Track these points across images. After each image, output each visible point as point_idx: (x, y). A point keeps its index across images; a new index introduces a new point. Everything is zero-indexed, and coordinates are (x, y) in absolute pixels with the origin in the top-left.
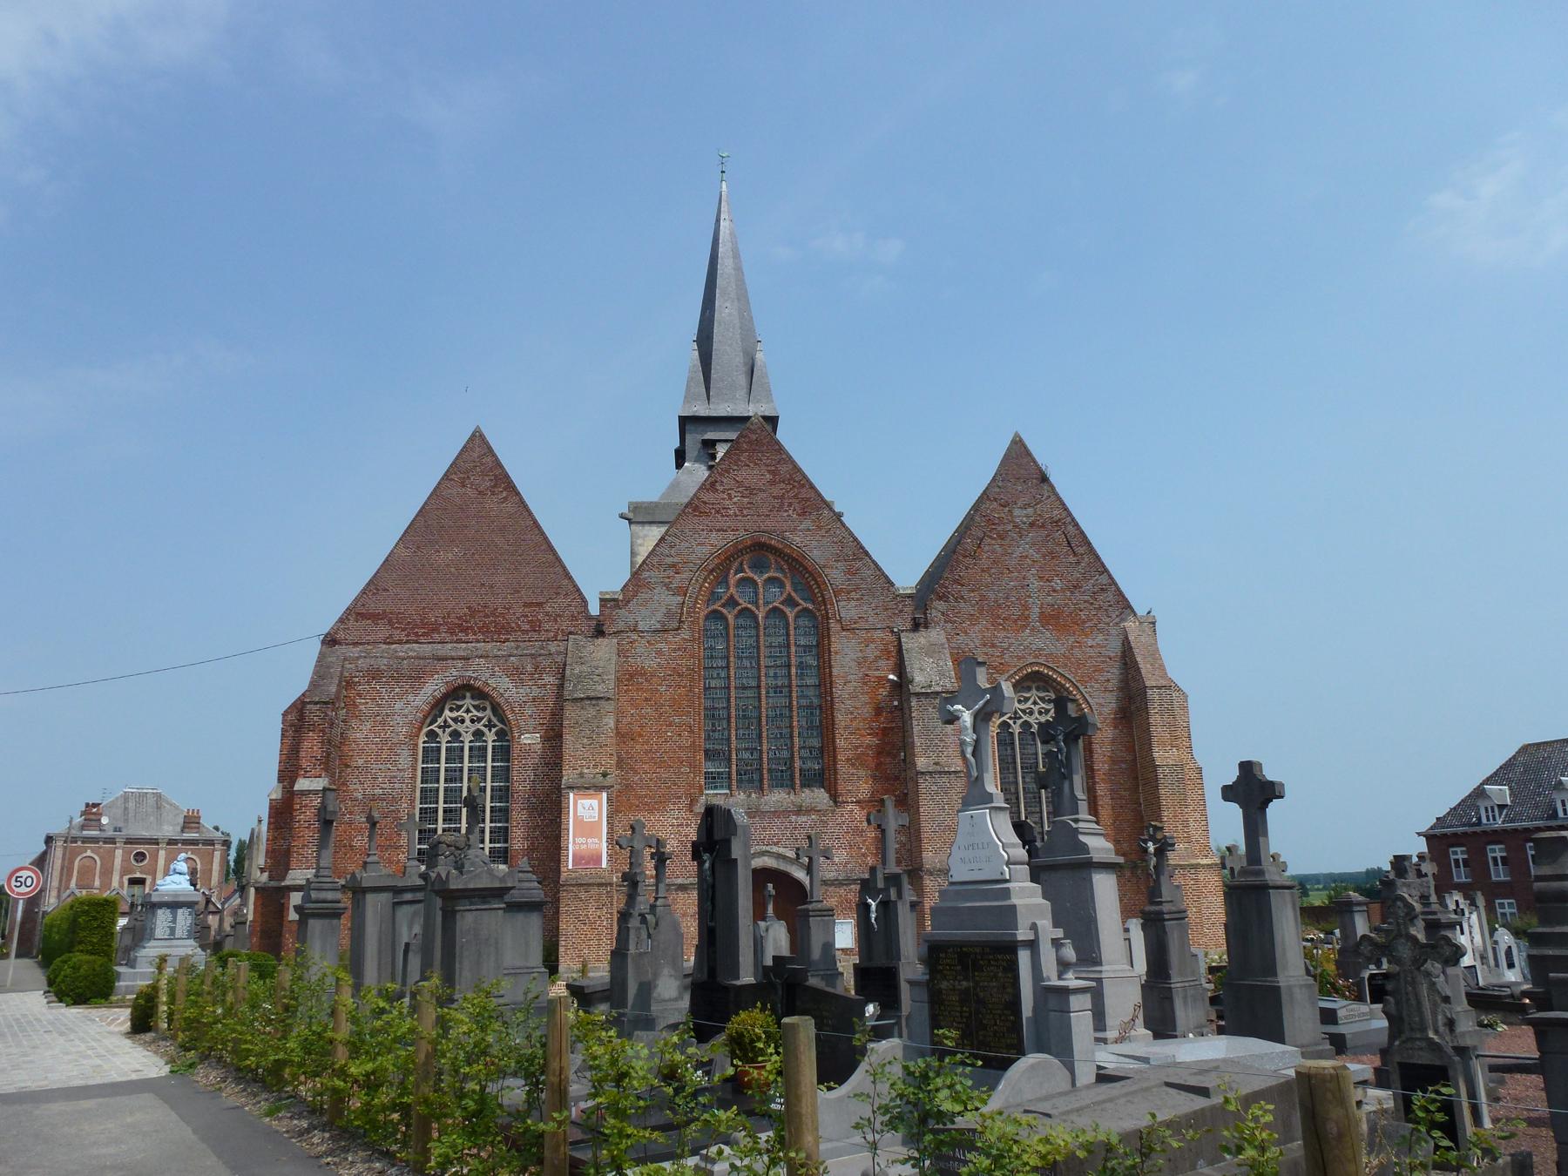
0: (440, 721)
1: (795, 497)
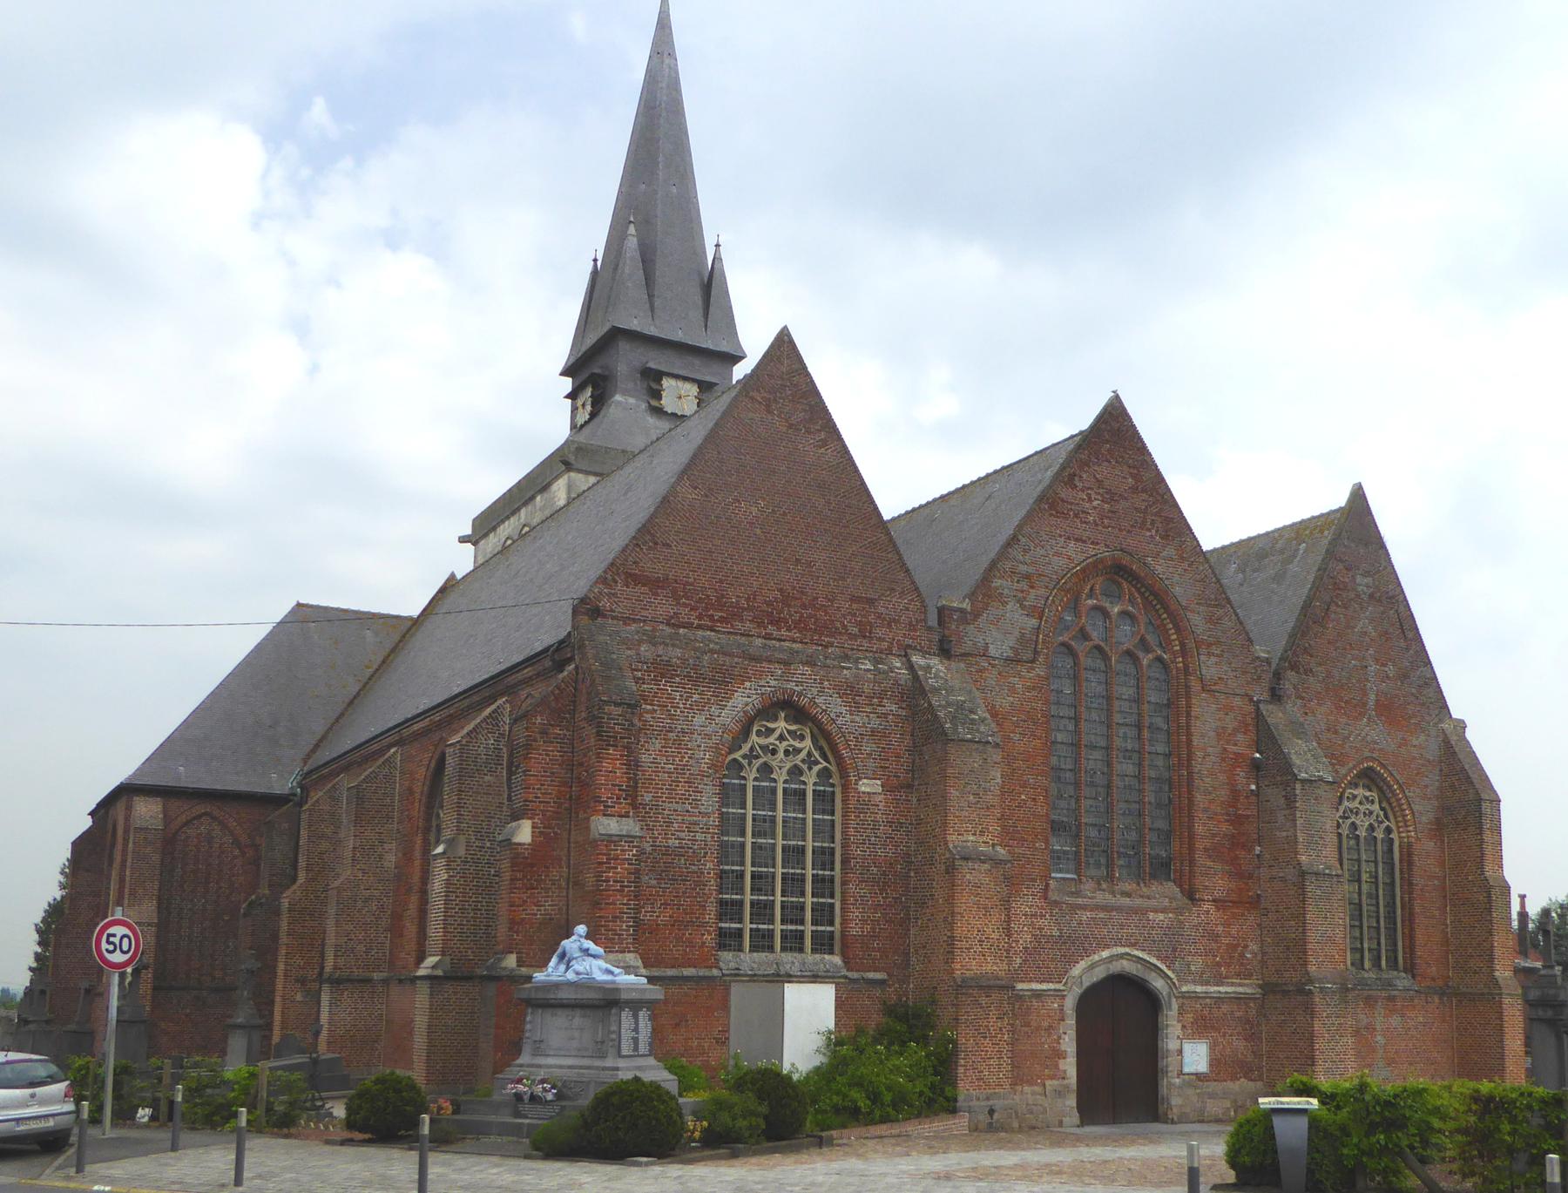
0: (746, 749)
1: (1158, 514)
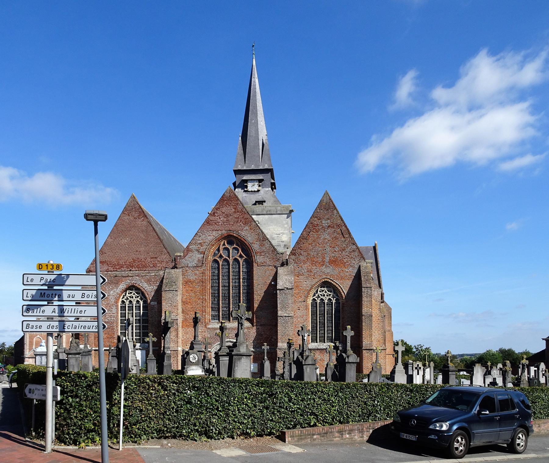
0: (125, 297)
